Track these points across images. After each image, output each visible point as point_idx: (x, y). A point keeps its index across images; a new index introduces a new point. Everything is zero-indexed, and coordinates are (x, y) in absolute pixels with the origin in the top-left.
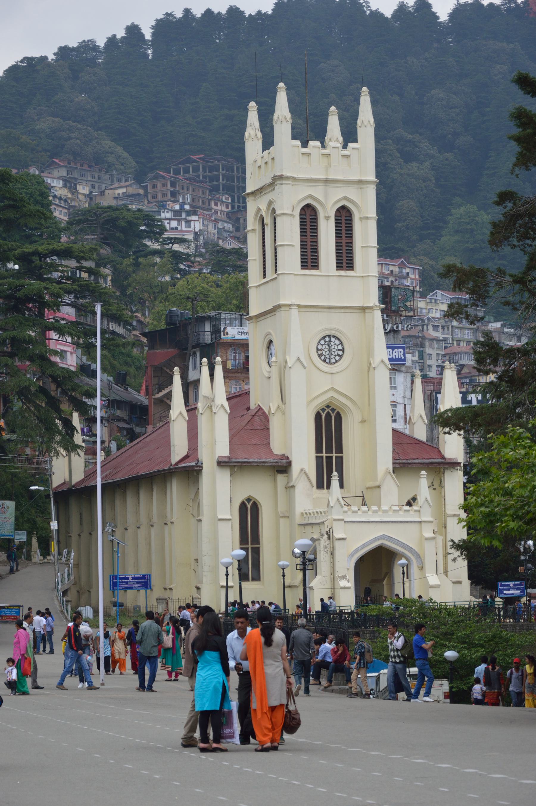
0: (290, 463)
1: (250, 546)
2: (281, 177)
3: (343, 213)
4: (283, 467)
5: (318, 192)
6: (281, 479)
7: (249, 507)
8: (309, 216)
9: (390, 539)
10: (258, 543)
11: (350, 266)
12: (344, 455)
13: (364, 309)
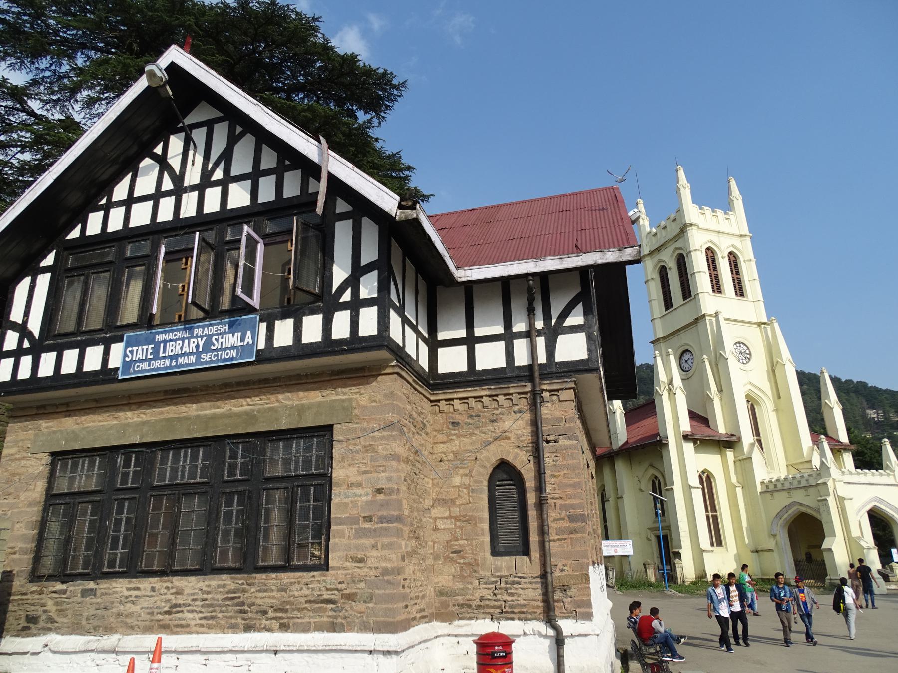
0: (740, 439)
1: (710, 514)
2: (691, 225)
3: (731, 256)
4: (730, 443)
5: (715, 238)
6: (730, 453)
7: (704, 477)
8: (711, 256)
9: (881, 500)
10: (716, 511)
11: (742, 295)
12: (762, 438)
13: (759, 324)
